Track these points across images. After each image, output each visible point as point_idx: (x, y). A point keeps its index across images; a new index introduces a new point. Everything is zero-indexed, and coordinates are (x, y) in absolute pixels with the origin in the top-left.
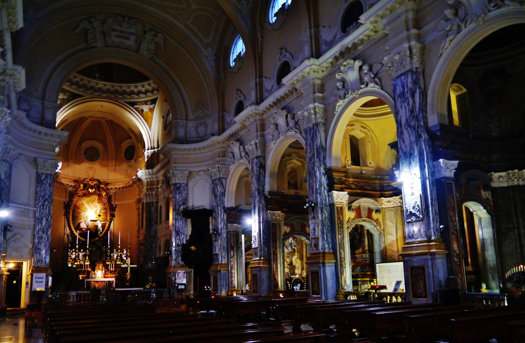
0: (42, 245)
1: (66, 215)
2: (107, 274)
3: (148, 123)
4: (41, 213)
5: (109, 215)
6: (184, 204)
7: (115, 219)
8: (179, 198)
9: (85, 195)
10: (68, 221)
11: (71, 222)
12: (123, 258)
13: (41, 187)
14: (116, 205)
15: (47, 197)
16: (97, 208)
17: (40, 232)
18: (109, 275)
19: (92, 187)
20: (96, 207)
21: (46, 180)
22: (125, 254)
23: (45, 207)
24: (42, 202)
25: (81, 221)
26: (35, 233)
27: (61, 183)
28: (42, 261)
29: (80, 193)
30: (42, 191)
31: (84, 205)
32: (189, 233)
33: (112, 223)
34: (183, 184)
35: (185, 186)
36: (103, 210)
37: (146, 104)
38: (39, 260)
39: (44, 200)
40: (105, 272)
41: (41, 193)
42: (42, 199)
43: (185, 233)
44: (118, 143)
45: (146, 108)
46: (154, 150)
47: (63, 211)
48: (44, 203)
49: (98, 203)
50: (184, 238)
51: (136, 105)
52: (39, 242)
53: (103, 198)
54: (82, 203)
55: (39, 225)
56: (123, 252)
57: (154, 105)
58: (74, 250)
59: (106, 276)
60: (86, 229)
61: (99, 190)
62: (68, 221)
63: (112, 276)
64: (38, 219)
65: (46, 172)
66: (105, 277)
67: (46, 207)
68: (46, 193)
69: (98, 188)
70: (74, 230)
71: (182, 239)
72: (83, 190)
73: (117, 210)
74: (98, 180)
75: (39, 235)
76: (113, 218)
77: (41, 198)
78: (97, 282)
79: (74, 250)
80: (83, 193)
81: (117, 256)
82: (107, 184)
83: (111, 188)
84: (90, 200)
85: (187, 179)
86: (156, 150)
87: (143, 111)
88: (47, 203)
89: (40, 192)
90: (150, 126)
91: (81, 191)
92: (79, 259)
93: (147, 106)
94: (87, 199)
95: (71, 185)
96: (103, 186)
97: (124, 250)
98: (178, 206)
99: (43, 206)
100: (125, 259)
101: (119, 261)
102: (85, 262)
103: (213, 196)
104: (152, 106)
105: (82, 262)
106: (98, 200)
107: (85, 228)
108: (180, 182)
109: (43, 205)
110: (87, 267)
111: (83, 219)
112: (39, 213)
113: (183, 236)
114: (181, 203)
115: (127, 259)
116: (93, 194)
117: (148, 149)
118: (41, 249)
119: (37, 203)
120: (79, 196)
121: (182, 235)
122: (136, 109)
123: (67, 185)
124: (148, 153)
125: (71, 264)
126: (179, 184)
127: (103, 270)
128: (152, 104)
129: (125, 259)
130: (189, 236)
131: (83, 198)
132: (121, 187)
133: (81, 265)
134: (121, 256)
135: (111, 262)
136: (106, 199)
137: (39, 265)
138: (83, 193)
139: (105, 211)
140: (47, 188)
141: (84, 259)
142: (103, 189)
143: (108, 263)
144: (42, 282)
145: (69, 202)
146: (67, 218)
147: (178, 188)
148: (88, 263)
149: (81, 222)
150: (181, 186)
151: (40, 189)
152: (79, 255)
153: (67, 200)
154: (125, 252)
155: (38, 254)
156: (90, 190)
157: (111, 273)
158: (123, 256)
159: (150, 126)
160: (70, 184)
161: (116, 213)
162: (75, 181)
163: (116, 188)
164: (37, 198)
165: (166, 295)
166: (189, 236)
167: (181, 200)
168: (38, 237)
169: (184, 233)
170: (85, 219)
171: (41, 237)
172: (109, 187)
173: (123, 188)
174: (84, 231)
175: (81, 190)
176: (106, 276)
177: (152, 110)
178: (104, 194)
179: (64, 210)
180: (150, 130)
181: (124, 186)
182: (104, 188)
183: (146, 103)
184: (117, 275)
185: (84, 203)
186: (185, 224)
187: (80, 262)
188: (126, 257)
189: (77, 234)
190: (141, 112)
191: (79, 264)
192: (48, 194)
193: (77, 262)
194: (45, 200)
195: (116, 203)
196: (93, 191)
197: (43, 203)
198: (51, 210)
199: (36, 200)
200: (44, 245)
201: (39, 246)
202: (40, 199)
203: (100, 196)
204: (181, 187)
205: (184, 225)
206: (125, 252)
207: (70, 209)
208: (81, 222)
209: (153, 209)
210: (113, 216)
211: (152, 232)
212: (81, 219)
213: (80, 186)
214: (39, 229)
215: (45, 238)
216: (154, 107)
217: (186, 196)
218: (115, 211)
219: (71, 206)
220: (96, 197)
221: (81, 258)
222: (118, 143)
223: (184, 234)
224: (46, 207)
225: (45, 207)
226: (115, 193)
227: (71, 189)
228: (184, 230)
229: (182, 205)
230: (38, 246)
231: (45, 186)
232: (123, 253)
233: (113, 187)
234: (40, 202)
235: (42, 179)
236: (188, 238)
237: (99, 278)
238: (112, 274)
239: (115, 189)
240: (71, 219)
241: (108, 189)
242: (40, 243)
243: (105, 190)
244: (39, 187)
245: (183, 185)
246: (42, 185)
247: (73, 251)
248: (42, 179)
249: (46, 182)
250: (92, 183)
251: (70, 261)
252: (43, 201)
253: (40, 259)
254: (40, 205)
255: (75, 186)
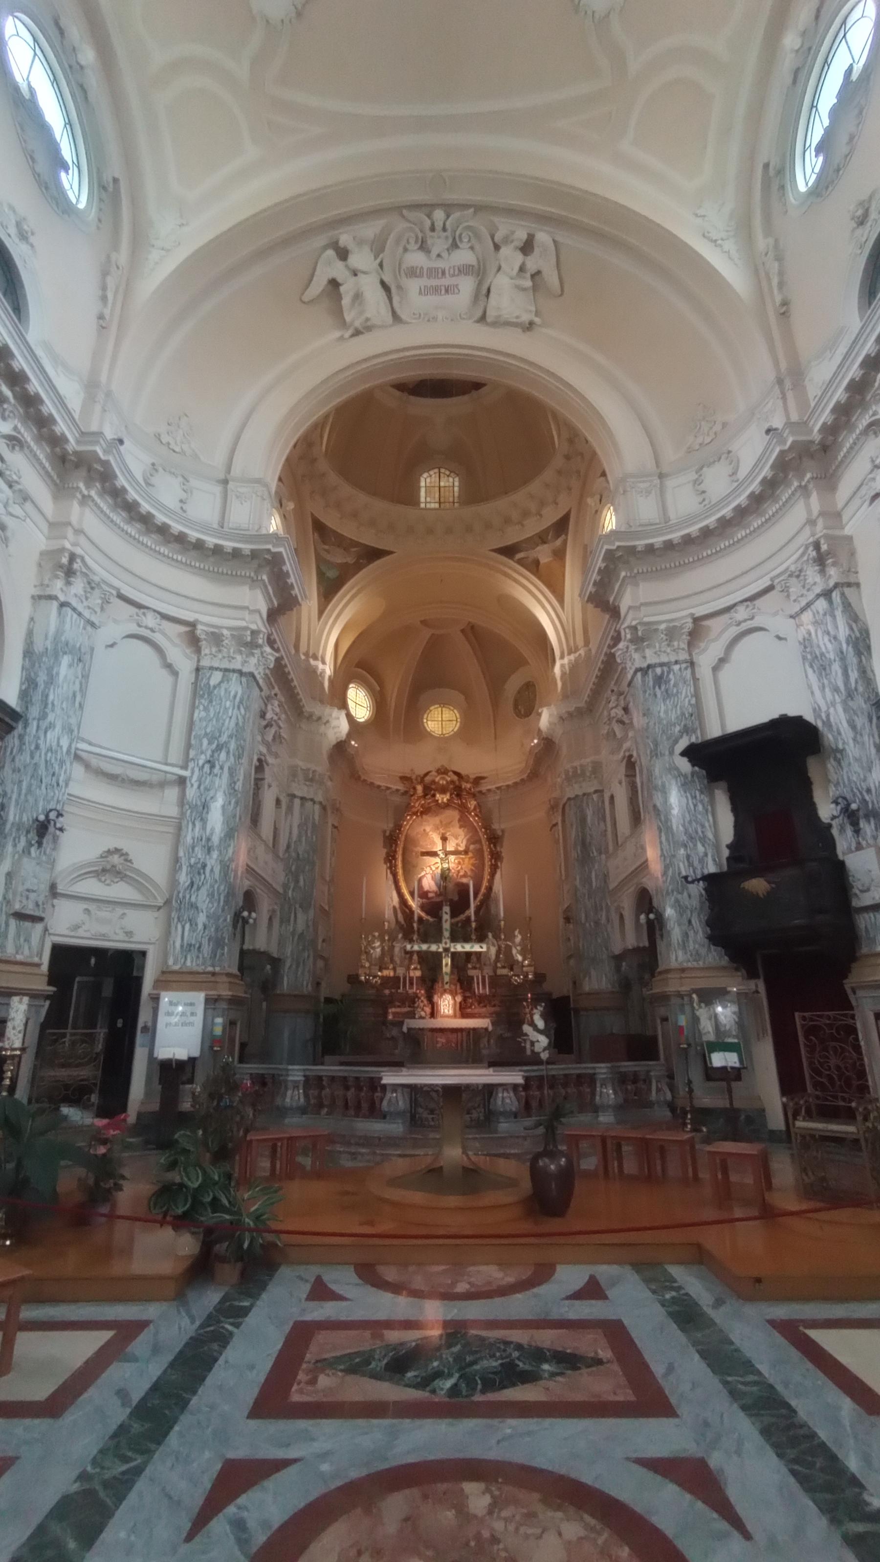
0: (203, 892)
1: (390, 859)
2: (470, 1007)
3: (553, 592)
4: (202, 787)
5: (487, 856)
6: (686, 730)
7: (505, 866)
8: (666, 712)
9: (426, 811)
10: (395, 875)
11: (401, 877)
12: (516, 958)
13: (206, 709)
14: (503, 831)
15: (224, 738)
16: (459, 841)
17: (196, 849)
18: (476, 1009)
19: (443, 791)
20: (457, 838)
21: (224, 686)
22: (520, 945)
23: (217, 767)
24: (209, 753)
25: (423, 874)
26: (181, 854)
27: (372, 784)
28: (200, 947)
29: (417, 805)
30: (211, 720)
31: (427, 834)
32: (727, 834)
33: (498, 876)
34: (676, 662)
35: (686, 668)
36: (473, 843)
37: (544, 542)
38: (190, 945)
39: (214, 746)
40: (465, 999)
41: (206, 726)
42: (210, 743)
43: (710, 835)
44: (496, 685)
45: (543, 554)
46: (577, 654)
47: (383, 852)
48: (216, 755)
49: (461, 827)
50: (706, 855)
51: (520, 551)
52: (192, 884)
53: (470, 814)
54: (424, 830)
55: (194, 824)
56: (510, 937)
57: (563, 536)
58: (377, 934)
59: (469, 1010)
60: (436, 893)
61: (459, 796)
62: (395, 875)
63: (484, 1010)
64: (193, 807)
65: (225, 665)
66: (464, 1015)
67: (222, 768)
68: (223, 724)
69: (458, 792)
70: (408, 897)
71: (701, 861)
72: (425, 796)
73: (506, 842)
74: (456, 773)
75: (193, 861)
76: (499, 864)
77: (205, 742)
78: (442, 1030)
79: (377, 934)
80: (422, 806)
81: (498, 952)
82: (478, 780)
83: (489, 790)
84: (441, 822)
85: (690, 644)
86: (582, 652)
87: (537, 563)
88: (223, 755)
89: (204, 724)
90: (561, 599)
91: (417, 800)
92: (392, 961)
93: (546, 546)
94: (436, 820)
95: (397, 790)
96: (468, 786)
97: (517, 933)
98: (668, 739)
99: (213, 767)
100: (520, 958)
101: (504, 967)
102: (408, 969)
103: (810, 671)
104: (559, 542)
105: (401, 971)
106: (459, 821)
107: (433, 892)
108: (664, 659)
109: (211, 763)
110: (411, 984)
111: (428, 870)
112: (196, 785)
113: (700, 848)
114: (678, 728)
115: (524, 959)
116: (447, 806)
117: (562, 657)
118: (197, 908)
119: (191, 756)
120: (415, 814)
121: (695, 845)
122: (520, 562)
123: (388, 788)
124: (562, 666)
125: (366, 974)
126: (662, 665)
127: (456, 994)
128: (558, 536)
129: (520, 958)
130: (728, 846)
131: (424, 816)
132: (510, 783)
133: (396, 979)
134: (509, 949)
135: (481, 969)
136: (476, 815)
137: (188, 963)
138: (422, 806)
139: (478, 846)
140: (226, 709)
141: (407, 962)
142: (469, 793)
143: (471, 973)
144: (191, 1024)
145: (393, 831)
146: (390, 868)
147: (659, 680)
148: (418, 973)
149: (424, 876)
150: (669, 673)
151: (203, 714)
152: (393, 947)
153: (391, 825)
154: (518, 939)
155: (187, 926)
156: (438, 796)
157: (479, 1003)
158: (514, 951)
159: (561, 601)
160: (394, 787)
161: (505, 850)
162: (404, 779)
163: (498, 788)
164: (193, 742)
165: (659, 1090)
166: (728, 846)
167: (677, 718)
168: (191, 866)
169: (705, 836)
170: (434, 869)
171: (199, 866)
172: (484, 788)
173: (516, 784)
174: (432, 898)
175: (419, 798)
176: (469, 1010)
177: (559, 555)
178: (472, 804)
179: (385, 851)
180: (563, 607)
181: (518, 780)
182: (470, 789)
183: (541, 538)
184: (497, 1009)
185: (428, 829)
186: (701, 801)
187: (394, 969)
188: (523, 953)
189: (413, 904)
190: (534, 567)
191: (392, 974)
192: (228, 729)
193: (387, 968)
194: (219, 748)
195: (503, 826)
196: (445, 800)
197: (212, 756)
198: (238, 780)
199: (189, 746)
200: (208, 895)
201: (193, 899)
202: (201, 745)
203: (463, 809)
204: (671, 676)
205: (700, 807)
206: (518, 939)
207: (396, 845)
208: (424, 876)
209: (589, 813)
210: (496, 857)
211: (594, 880)
212: (423, 869)
213: (415, 788)
214: (193, 838)
215: (212, 870)
216: (565, 542)
217: (693, 701)
218: (502, 847)
219: (398, 838)
220: (454, 814)
221: (397, 960)
222: (496, 685)
223: (704, 840)
224: (222, 768)
225: (217, 770)
226: (500, 799)
227: (397, 799)
228: (703, 826)
229: (681, 737)
230: (188, 896)
231: (221, 704)
232: (513, 942)
233: (493, 787)
234: (202, 753)
235: (212, 683)
236: (726, 853)
237: (448, 1016)
238: (485, 1006)
239: (498, 792)
240: (400, 871)
241: (480, 792)
242: (195, 887)
243: (474, 796)
244: (201, 707)
245: (676, 668)
246: (211, 701)
247: (374, 936)
248: (212, 683)
249: (222, 693)
250: (443, 779)
251: (364, 967)
252: (213, 752)
253: (193, 942)
254: (201, 762)
255: (406, 793)
